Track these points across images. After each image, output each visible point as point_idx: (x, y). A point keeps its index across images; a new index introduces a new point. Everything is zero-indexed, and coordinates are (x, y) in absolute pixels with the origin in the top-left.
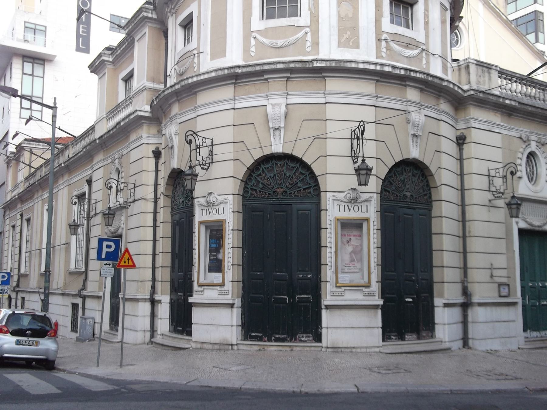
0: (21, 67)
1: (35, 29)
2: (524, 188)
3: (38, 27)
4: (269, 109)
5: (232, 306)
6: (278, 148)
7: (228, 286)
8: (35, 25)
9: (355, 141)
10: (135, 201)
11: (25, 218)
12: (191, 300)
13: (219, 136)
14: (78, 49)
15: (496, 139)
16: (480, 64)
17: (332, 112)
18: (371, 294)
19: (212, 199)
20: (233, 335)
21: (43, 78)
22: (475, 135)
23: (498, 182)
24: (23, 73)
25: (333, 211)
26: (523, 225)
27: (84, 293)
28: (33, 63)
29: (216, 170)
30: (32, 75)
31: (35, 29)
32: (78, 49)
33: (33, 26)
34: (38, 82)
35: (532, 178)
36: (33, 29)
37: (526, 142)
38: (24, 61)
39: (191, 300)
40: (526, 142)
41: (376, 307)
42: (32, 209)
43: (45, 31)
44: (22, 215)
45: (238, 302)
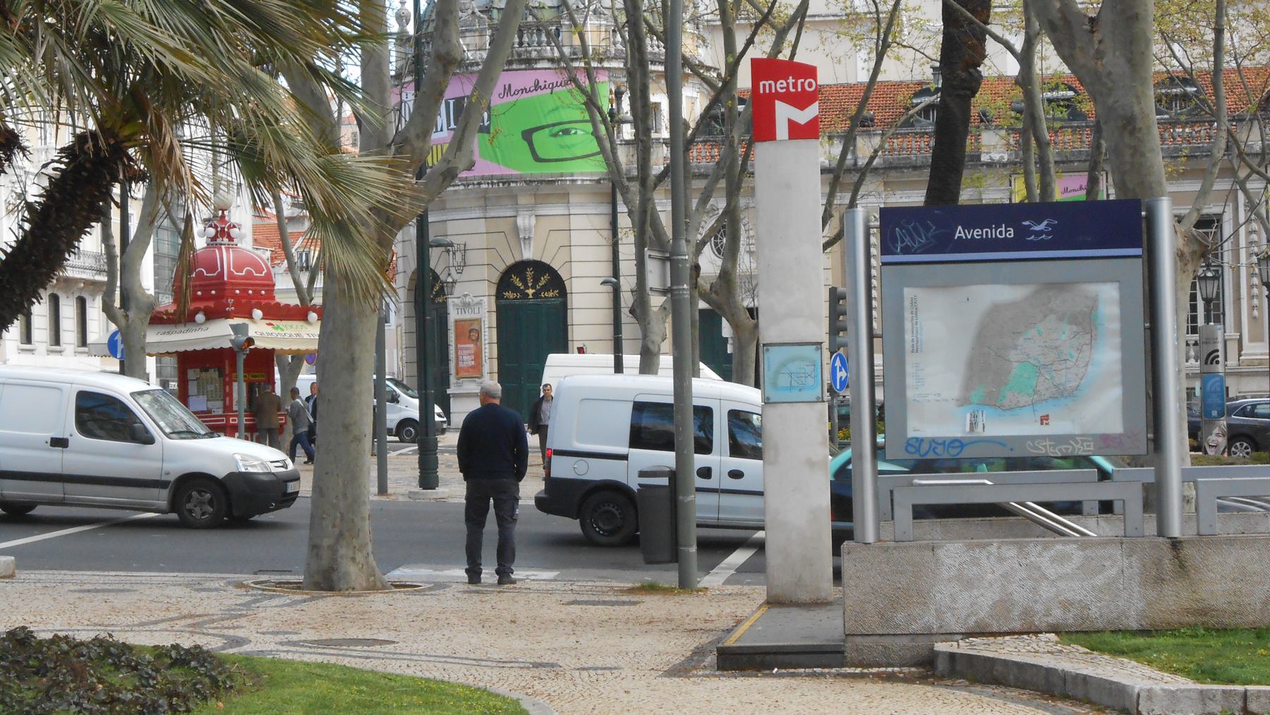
4: (520, 221)
12: (449, 391)
19: (468, 299)
29: (469, 273)
39: (449, 391)
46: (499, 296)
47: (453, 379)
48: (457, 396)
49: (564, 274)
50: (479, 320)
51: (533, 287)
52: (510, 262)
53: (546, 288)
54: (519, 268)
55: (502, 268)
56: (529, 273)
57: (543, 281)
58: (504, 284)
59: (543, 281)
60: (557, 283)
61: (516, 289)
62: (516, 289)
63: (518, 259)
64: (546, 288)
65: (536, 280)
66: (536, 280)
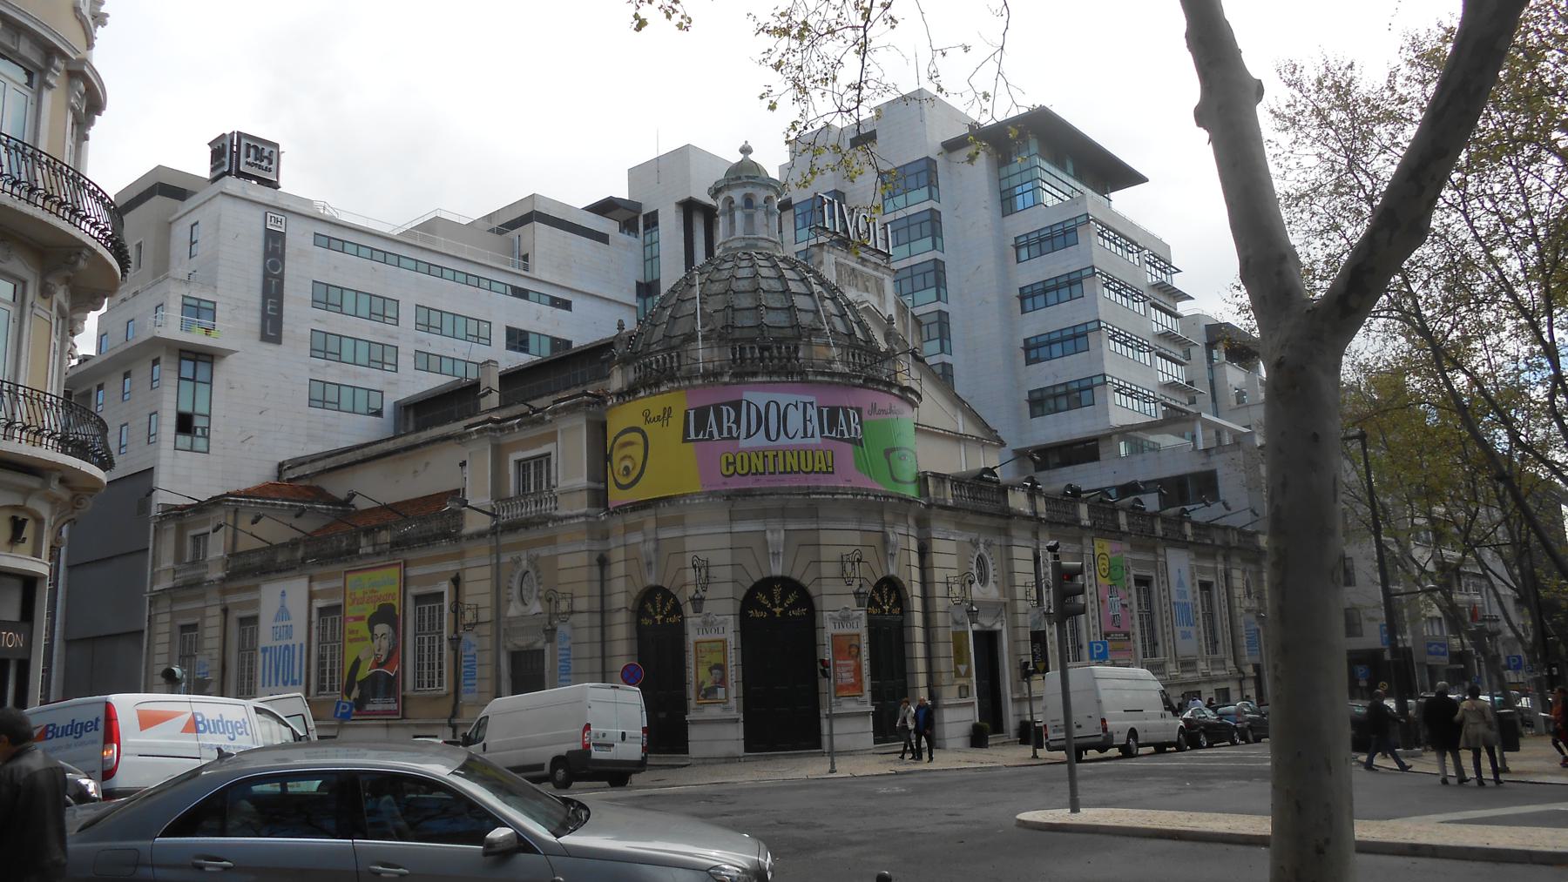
0: (175, 367)
1: (198, 307)
2: (977, 591)
3: (203, 304)
5: (737, 721)
6: (777, 570)
7: (733, 703)
8: (199, 300)
9: (848, 566)
10: (572, 612)
11: (235, 614)
13: (714, 559)
14: (265, 338)
15: (950, 547)
16: (936, 476)
17: (825, 537)
18: (864, 702)
20: (739, 748)
21: (211, 383)
22: (937, 545)
23: (956, 588)
24: (180, 378)
25: (829, 628)
26: (976, 627)
27: (457, 721)
28: (195, 361)
30: (194, 380)
31: (198, 307)
32: (265, 338)
33: (195, 303)
34: (202, 390)
35: (983, 580)
36: (197, 310)
37: (975, 544)
38: (181, 358)
40: (975, 544)
41: (867, 714)
42: (256, 603)
43: (214, 311)
44: (225, 611)
45: (741, 716)
46: (743, 616)
47: (692, 703)
48: (693, 722)
49: (813, 591)
50: (724, 642)
51: (781, 605)
52: (757, 577)
53: (793, 606)
54: (766, 584)
55: (749, 585)
56: (777, 590)
57: (791, 599)
58: (749, 602)
59: (791, 599)
60: (806, 599)
61: (762, 607)
62: (762, 607)
63: (766, 575)
64: (793, 606)
65: (784, 597)
66: (784, 597)
